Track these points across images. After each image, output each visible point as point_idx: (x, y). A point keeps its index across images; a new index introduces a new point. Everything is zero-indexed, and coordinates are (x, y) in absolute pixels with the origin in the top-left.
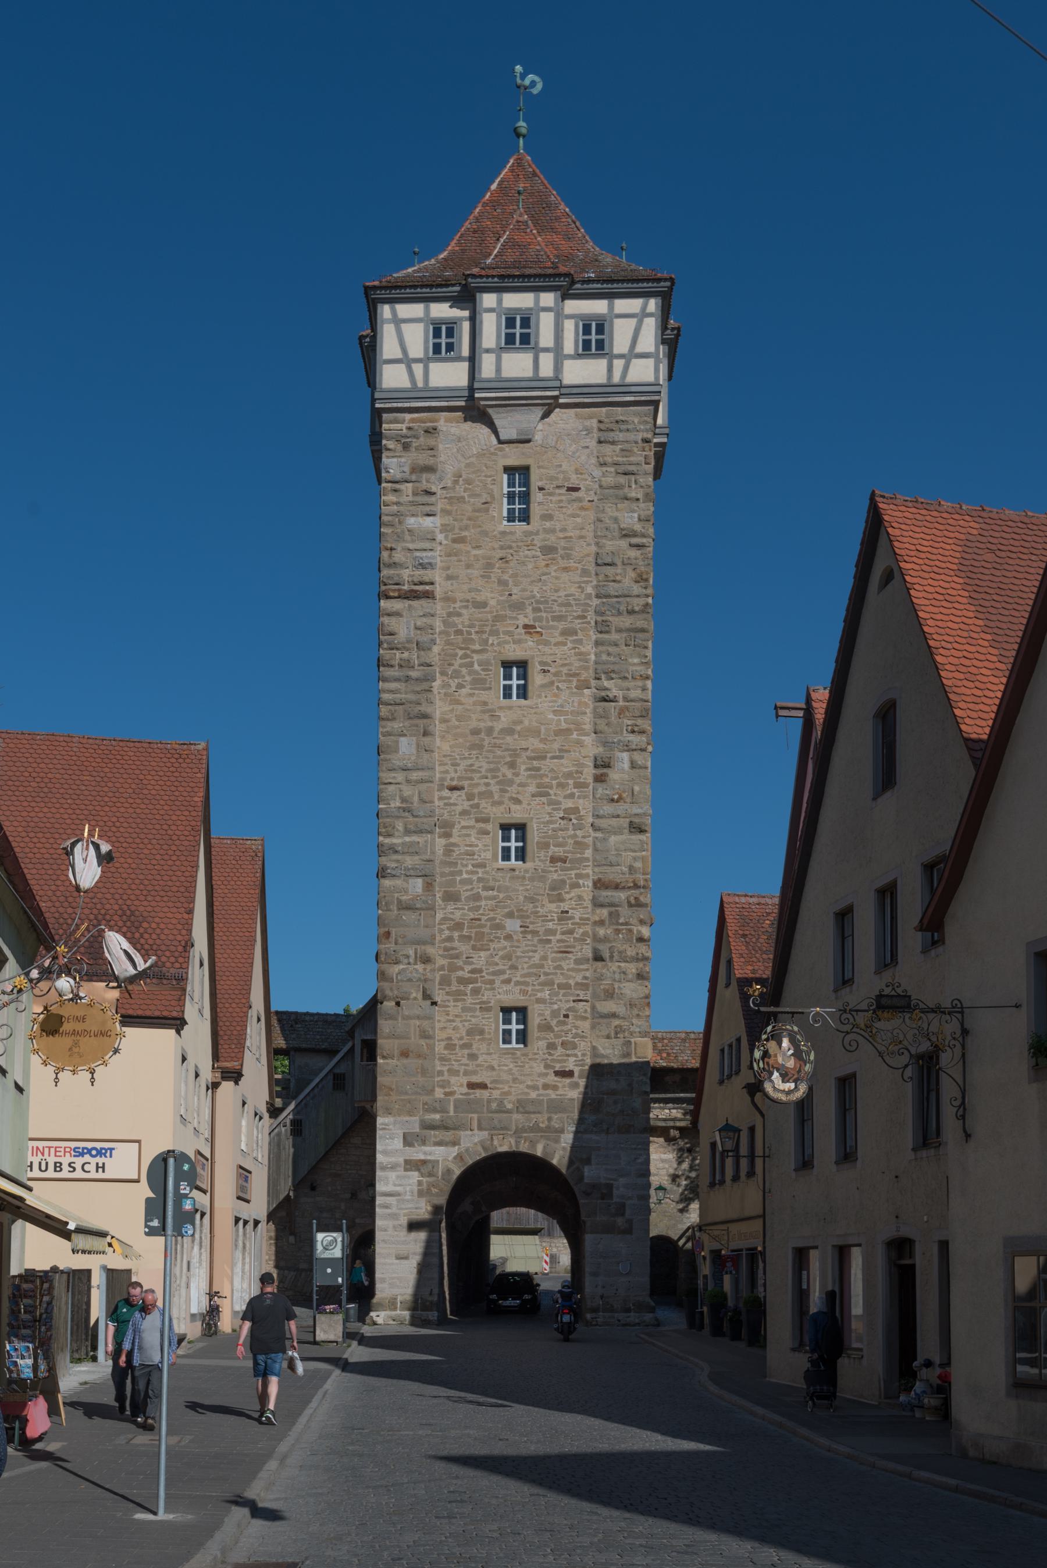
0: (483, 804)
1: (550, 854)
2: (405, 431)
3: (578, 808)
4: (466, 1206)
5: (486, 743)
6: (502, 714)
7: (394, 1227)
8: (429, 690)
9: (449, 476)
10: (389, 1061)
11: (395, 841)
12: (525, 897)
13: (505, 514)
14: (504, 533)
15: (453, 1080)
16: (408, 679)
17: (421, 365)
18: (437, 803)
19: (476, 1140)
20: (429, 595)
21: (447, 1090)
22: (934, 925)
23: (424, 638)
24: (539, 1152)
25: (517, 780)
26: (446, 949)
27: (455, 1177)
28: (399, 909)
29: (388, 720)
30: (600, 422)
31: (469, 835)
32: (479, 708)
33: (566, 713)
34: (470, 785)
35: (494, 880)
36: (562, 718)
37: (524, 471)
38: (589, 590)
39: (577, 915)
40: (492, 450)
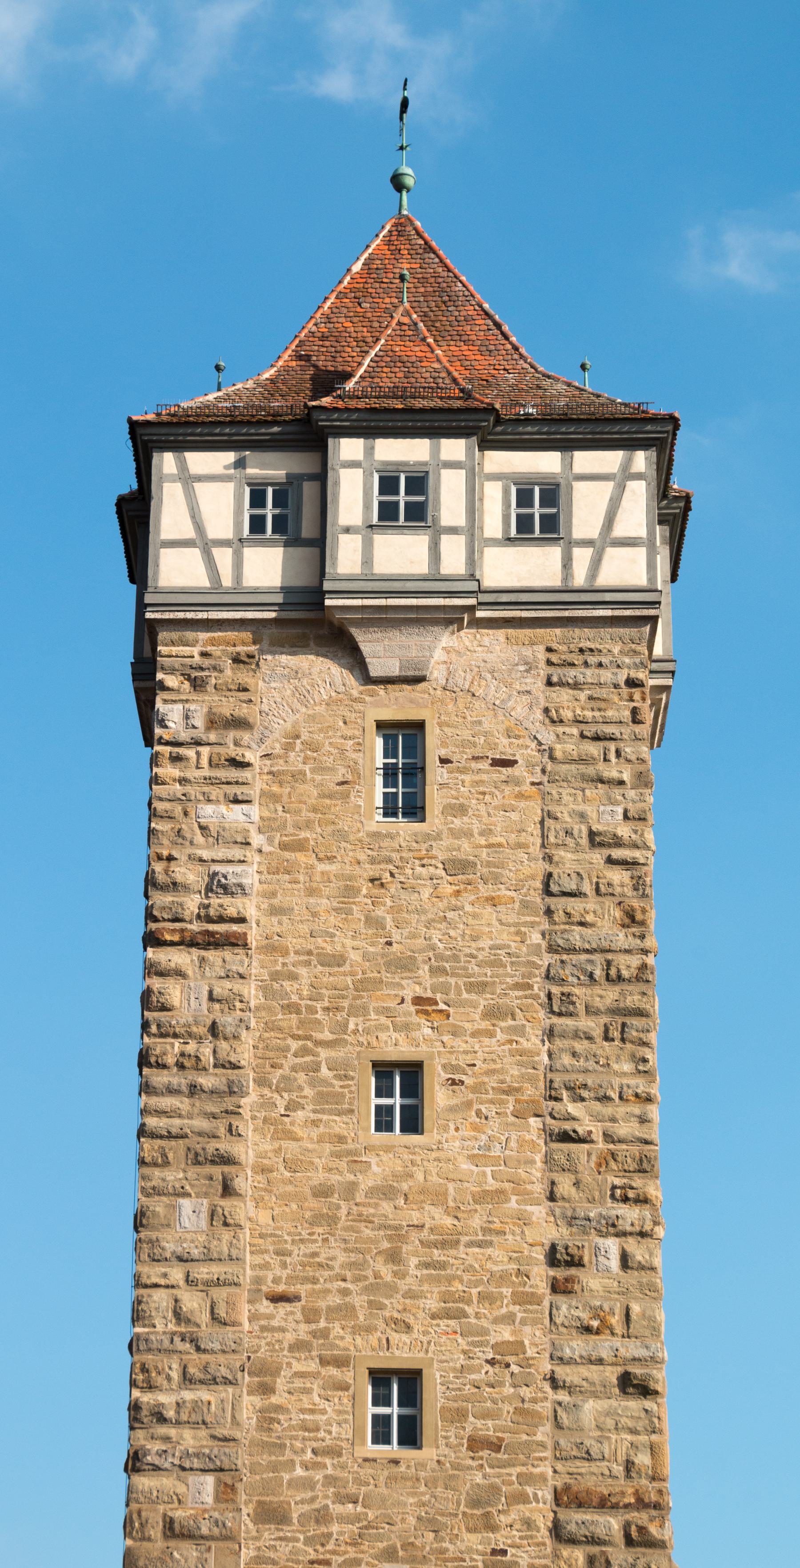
2: (197, 658)
6: (373, 1160)
9: (277, 735)
13: (379, 802)
14: (376, 835)
16: (194, 1090)
18: (246, 1326)
20: (236, 942)
28: (166, 1537)
30: (549, 650)
32: (328, 1148)
36: (488, 1170)
37: (414, 730)
38: (536, 938)
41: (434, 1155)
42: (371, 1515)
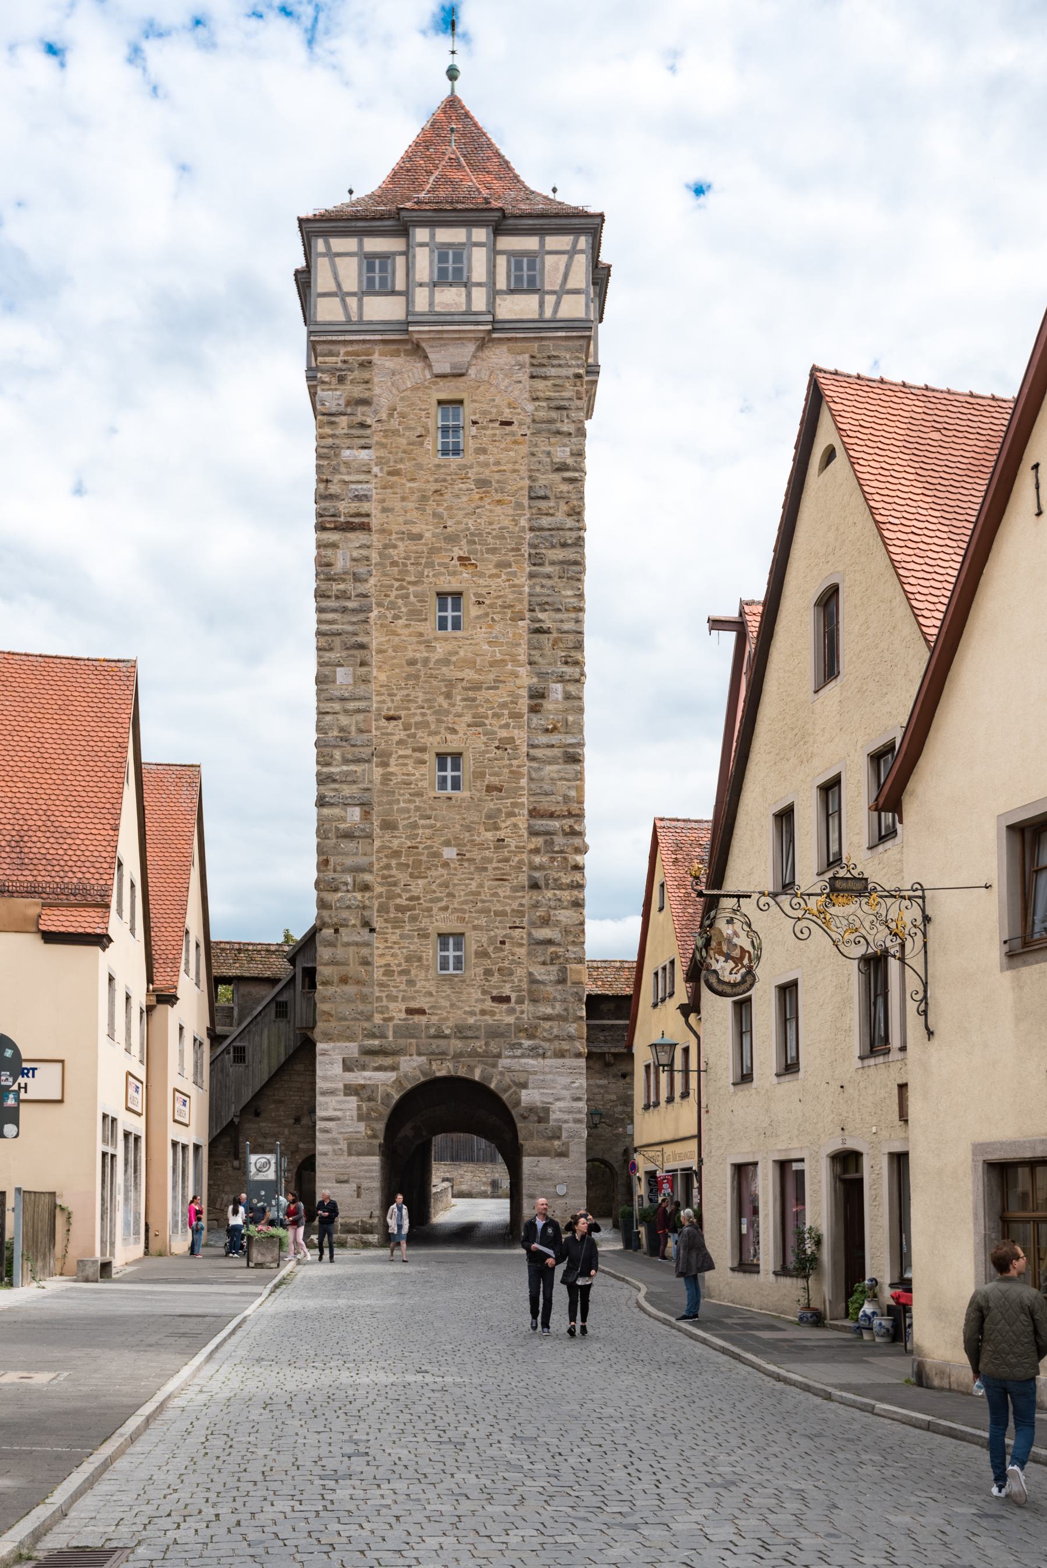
1: (486, 783)
4: (407, 1131)
5: (422, 673)
7: (334, 1151)
8: (366, 621)
10: (329, 987)
11: (333, 769)
14: (438, 466)
15: (392, 1006)
16: (344, 610)
17: (355, 299)
18: (374, 732)
19: (415, 1064)
20: (365, 528)
21: (386, 1016)
22: (890, 800)
23: (362, 570)
24: (477, 1077)
25: (453, 710)
26: (384, 877)
27: (394, 1101)
28: (337, 837)
29: (325, 650)
30: (533, 357)
31: (406, 765)
32: (415, 639)
33: (502, 644)
34: (407, 716)
35: (433, 809)
38: (523, 522)
39: (513, 844)
41: (469, 642)
42: (438, 824)
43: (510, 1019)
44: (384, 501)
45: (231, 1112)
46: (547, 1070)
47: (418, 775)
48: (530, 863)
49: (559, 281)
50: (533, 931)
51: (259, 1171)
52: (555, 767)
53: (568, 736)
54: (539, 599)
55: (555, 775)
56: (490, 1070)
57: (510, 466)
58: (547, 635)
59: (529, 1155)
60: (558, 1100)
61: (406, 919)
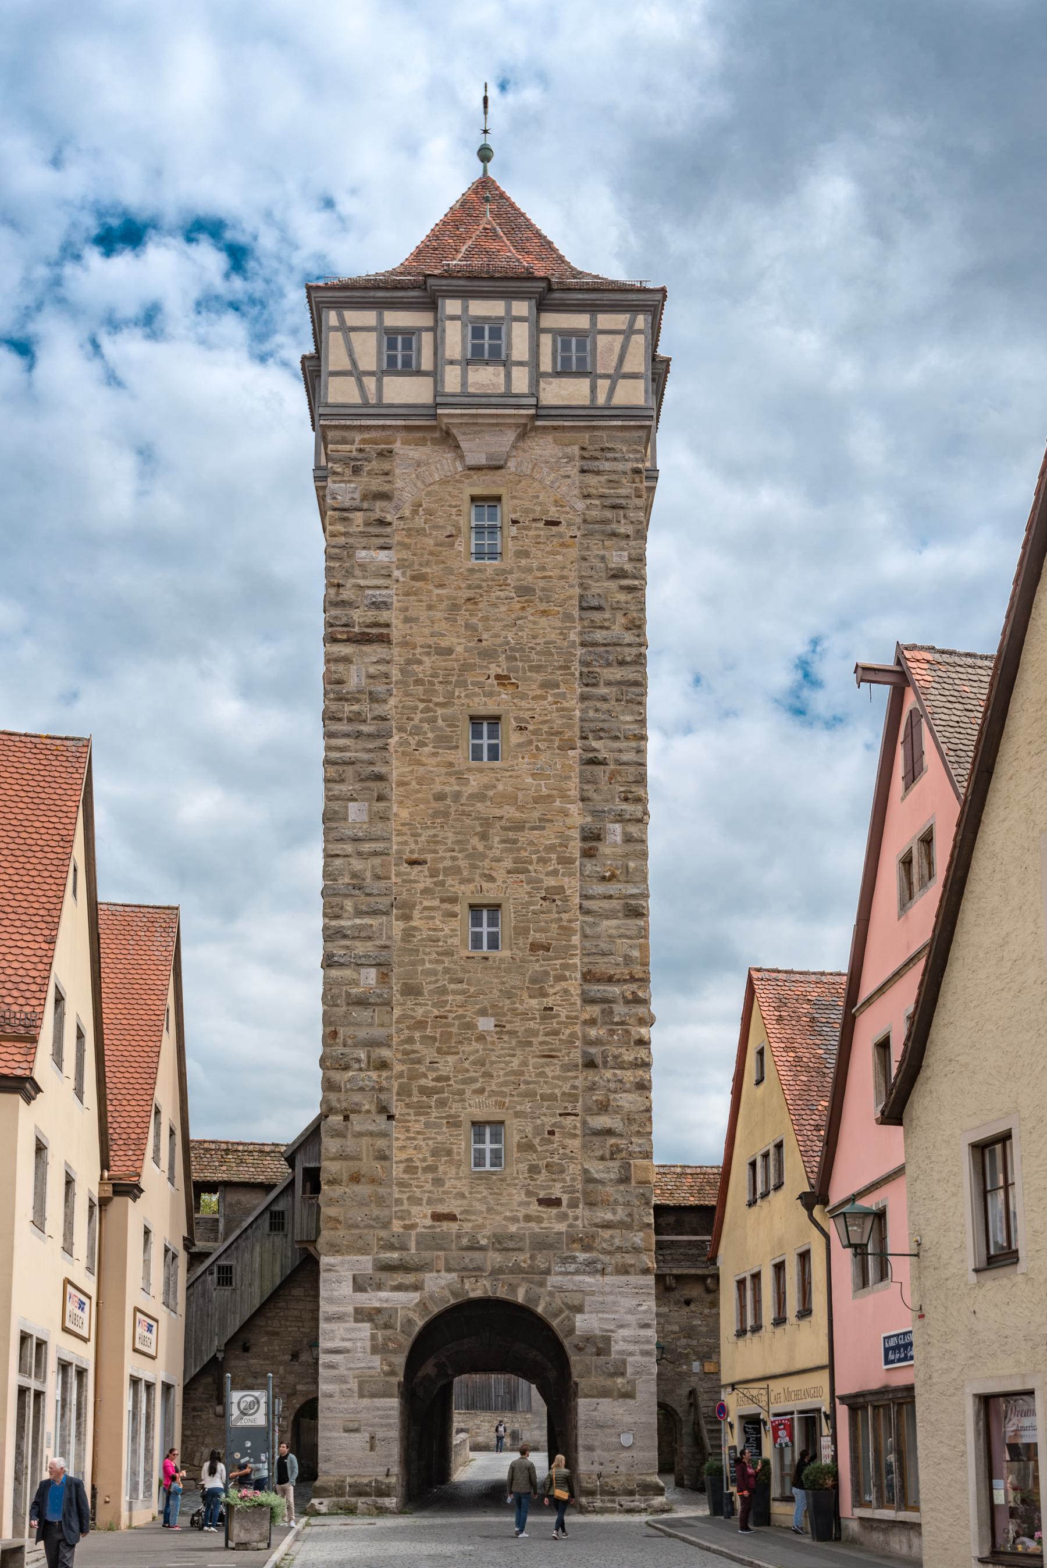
0: (449, 881)
1: (530, 940)
3: (563, 887)
5: (452, 810)
7: (341, 1391)
8: (384, 748)
9: (407, 505)
10: (337, 1187)
11: (343, 923)
12: (501, 991)
14: (472, 570)
15: (415, 1210)
16: (359, 735)
18: (394, 879)
19: (443, 1283)
20: (384, 640)
21: (407, 1222)
23: (380, 688)
24: (520, 1298)
25: (490, 854)
26: (406, 1053)
27: (417, 1329)
28: (348, 1004)
29: (335, 781)
30: (583, 449)
31: (433, 918)
32: (444, 770)
33: (548, 777)
34: (434, 860)
38: (573, 636)
39: (564, 1013)
40: (457, 476)
41: (508, 774)
42: (472, 990)
43: (562, 1227)
44: (406, 609)
45: (214, 1346)
46: (607, 1289)
47: (447, 931)
48: (584, 1036)
49: (614, 364)
50: (589, 1119)
51: (243, 1413)
52: (614, 922)
53: (629, 886)
54: (592, 725)
55: (614, 932)
56: (537, 1290)
57: (556, 572)
58: (602, 767)
59: (586, 1396)
60: (621, 1326)
61: (433, 1104)
